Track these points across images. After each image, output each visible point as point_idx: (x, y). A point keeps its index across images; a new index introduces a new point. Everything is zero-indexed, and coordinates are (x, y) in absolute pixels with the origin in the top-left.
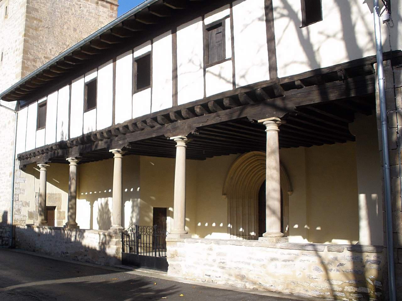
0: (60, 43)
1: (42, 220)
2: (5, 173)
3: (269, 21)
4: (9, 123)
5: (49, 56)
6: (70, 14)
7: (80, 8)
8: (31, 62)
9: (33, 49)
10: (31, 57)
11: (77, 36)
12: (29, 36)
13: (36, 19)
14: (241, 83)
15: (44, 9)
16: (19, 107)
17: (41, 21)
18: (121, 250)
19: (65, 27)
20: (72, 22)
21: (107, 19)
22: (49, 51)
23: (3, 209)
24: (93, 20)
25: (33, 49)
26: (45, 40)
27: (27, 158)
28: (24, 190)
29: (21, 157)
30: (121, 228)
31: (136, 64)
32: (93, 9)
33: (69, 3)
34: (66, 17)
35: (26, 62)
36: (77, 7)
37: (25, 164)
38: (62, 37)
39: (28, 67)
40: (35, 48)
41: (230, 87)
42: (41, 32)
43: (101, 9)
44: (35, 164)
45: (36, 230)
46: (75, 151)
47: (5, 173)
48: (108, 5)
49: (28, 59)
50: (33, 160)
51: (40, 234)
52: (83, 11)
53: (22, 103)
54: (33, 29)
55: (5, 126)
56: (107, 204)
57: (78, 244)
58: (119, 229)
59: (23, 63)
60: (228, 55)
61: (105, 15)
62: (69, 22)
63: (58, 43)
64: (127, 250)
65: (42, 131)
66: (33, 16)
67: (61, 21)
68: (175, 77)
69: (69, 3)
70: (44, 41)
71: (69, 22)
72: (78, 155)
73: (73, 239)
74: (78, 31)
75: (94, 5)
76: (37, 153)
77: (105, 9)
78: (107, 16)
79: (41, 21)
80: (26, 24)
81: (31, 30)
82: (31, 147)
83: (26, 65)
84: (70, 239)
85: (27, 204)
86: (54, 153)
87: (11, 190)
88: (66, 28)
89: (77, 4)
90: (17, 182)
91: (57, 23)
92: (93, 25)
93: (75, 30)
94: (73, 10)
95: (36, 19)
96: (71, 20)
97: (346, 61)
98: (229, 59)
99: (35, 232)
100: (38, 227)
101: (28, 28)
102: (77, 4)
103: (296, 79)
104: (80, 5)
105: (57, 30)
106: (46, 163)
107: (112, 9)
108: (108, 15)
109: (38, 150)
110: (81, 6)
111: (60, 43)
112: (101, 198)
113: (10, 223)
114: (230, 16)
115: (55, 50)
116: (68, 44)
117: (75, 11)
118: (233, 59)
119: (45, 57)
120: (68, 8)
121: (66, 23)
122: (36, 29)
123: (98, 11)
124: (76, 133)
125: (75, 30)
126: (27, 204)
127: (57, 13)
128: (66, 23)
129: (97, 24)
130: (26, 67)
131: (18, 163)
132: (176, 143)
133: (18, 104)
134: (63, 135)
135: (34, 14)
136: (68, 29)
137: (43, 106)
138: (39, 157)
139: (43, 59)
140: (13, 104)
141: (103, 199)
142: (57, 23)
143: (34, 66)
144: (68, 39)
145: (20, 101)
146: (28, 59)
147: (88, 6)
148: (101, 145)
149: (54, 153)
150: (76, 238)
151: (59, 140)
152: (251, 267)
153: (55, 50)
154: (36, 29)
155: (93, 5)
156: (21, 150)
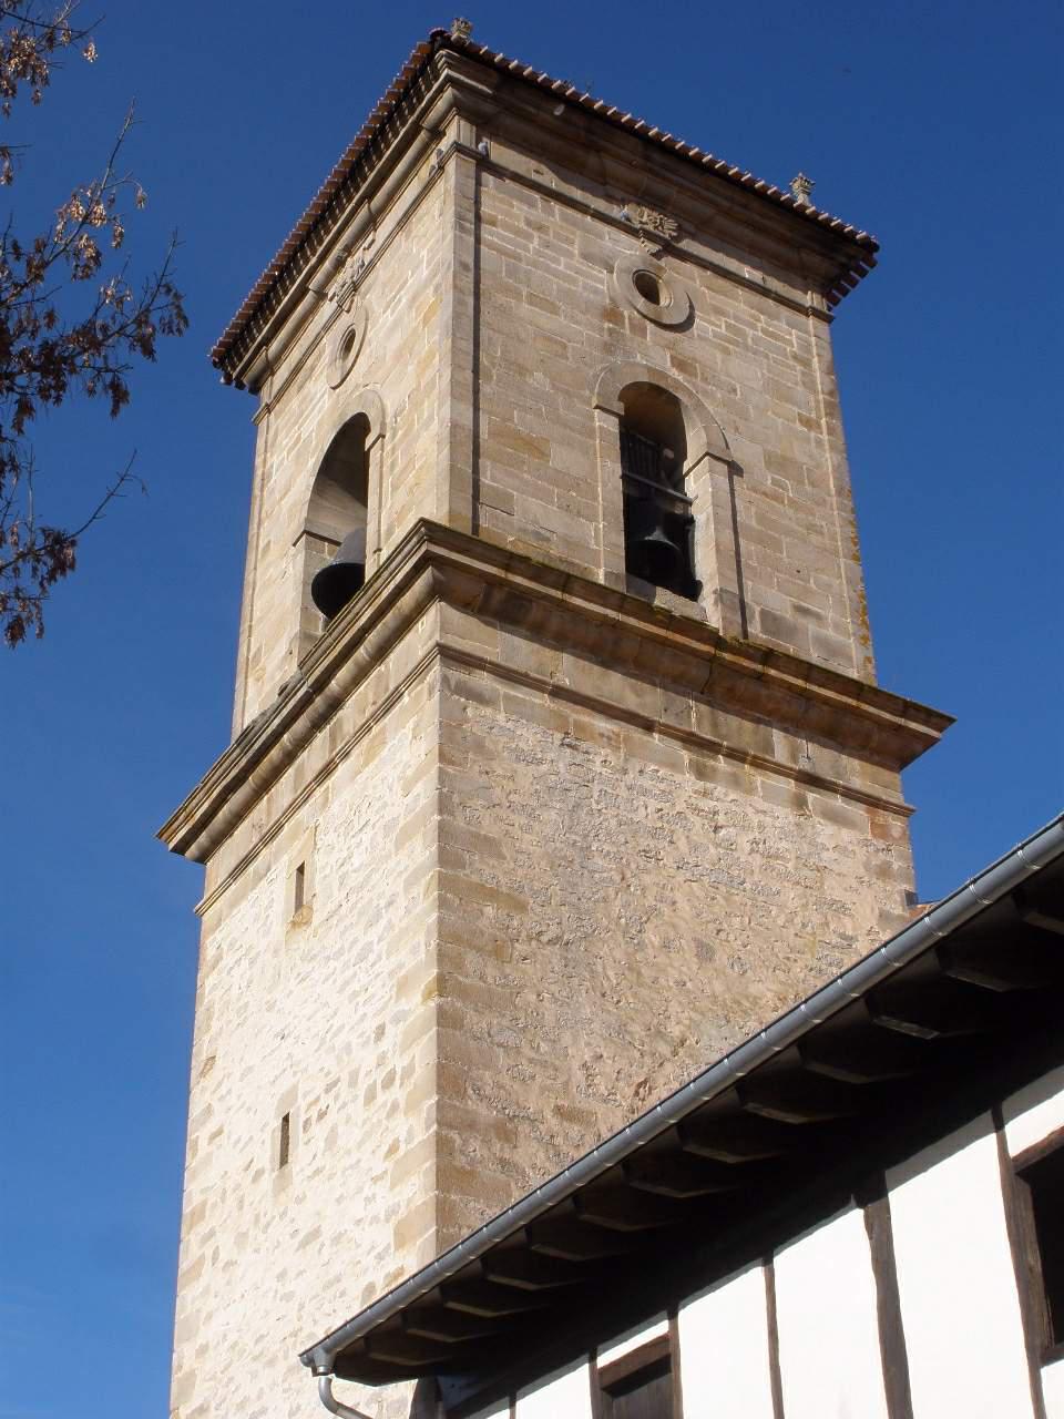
0: (637, 1029)
5: (582, 1103)
6: (669, 861)
7: (716, 829)
8: (486, 1142)
9: (488, 1065)
10: (485, 1113)
11: (718, 987)
12: (464, 993)
13: (493, 895)
15: (528, 842)
17: (522, 907)
19: (652, 937)
20: (683, 905)
21: (864, 890)
22: (579, 1075)
24: (791, 896)
25: (488, 1065)
26: (550, 1011)
32: (784, 835)
33: (653, 804)
34: (647, 879)
35: (458, 1141)
36: (698, 826)
38: (644, 992)
39: (472, 1174)
40: (502, 1060)
42: (527, 966)
43: (826, 832)
48: (858, 811)
49: (470, 1125)
52: (731, 846)
54: (479, 950)
59: (442, 1146)
61: (853, 866)
62: (666, 909)
63: (622, 1029)
66: (475, 878)
67: (626, 905)
69: (653, 804)
70: (549, 1018)
71: (666, 909)
74: (721, 958)
77: (846, 835)
78: (862, 871)
79: (522, 907)
80: (441, 921)
81: (472, 961)
83: (461, 1161)
88: (656, 941)
89: (697, 810)
91: (608, 916)
92: (798, 920)
93: (705, 952)
94: (682, 844)
95: (493, 895)
96: (678, 896)
101: (453, 945)
102: (697, 810)
104: (715, 813)
105: (612, 952)
107: (881, 831)
108: (867, 866)
110: (721, 819)
111: (637, 1029)
115: (608, 1067)
116: (675, 1031)
117: (695, 848)
119: (558, 1110)
120: (654, 833)
121: (652, 912)
122: (498, 951)
123: (812, 843)
125: (705, 952)
127: (600, 862)
128: (652, 912)
129: (816, 919)
130: (462, 1172)
135: (483, 870)
136: (666, 946)
139: (553, 1122)
142: (608, 916)
143: (503, 1163)
144: (674, 1008)
145: (444, 1381)
146: (470, 1125)
147: (755, 819)
153: (608, 1067)
154: (498, 951)
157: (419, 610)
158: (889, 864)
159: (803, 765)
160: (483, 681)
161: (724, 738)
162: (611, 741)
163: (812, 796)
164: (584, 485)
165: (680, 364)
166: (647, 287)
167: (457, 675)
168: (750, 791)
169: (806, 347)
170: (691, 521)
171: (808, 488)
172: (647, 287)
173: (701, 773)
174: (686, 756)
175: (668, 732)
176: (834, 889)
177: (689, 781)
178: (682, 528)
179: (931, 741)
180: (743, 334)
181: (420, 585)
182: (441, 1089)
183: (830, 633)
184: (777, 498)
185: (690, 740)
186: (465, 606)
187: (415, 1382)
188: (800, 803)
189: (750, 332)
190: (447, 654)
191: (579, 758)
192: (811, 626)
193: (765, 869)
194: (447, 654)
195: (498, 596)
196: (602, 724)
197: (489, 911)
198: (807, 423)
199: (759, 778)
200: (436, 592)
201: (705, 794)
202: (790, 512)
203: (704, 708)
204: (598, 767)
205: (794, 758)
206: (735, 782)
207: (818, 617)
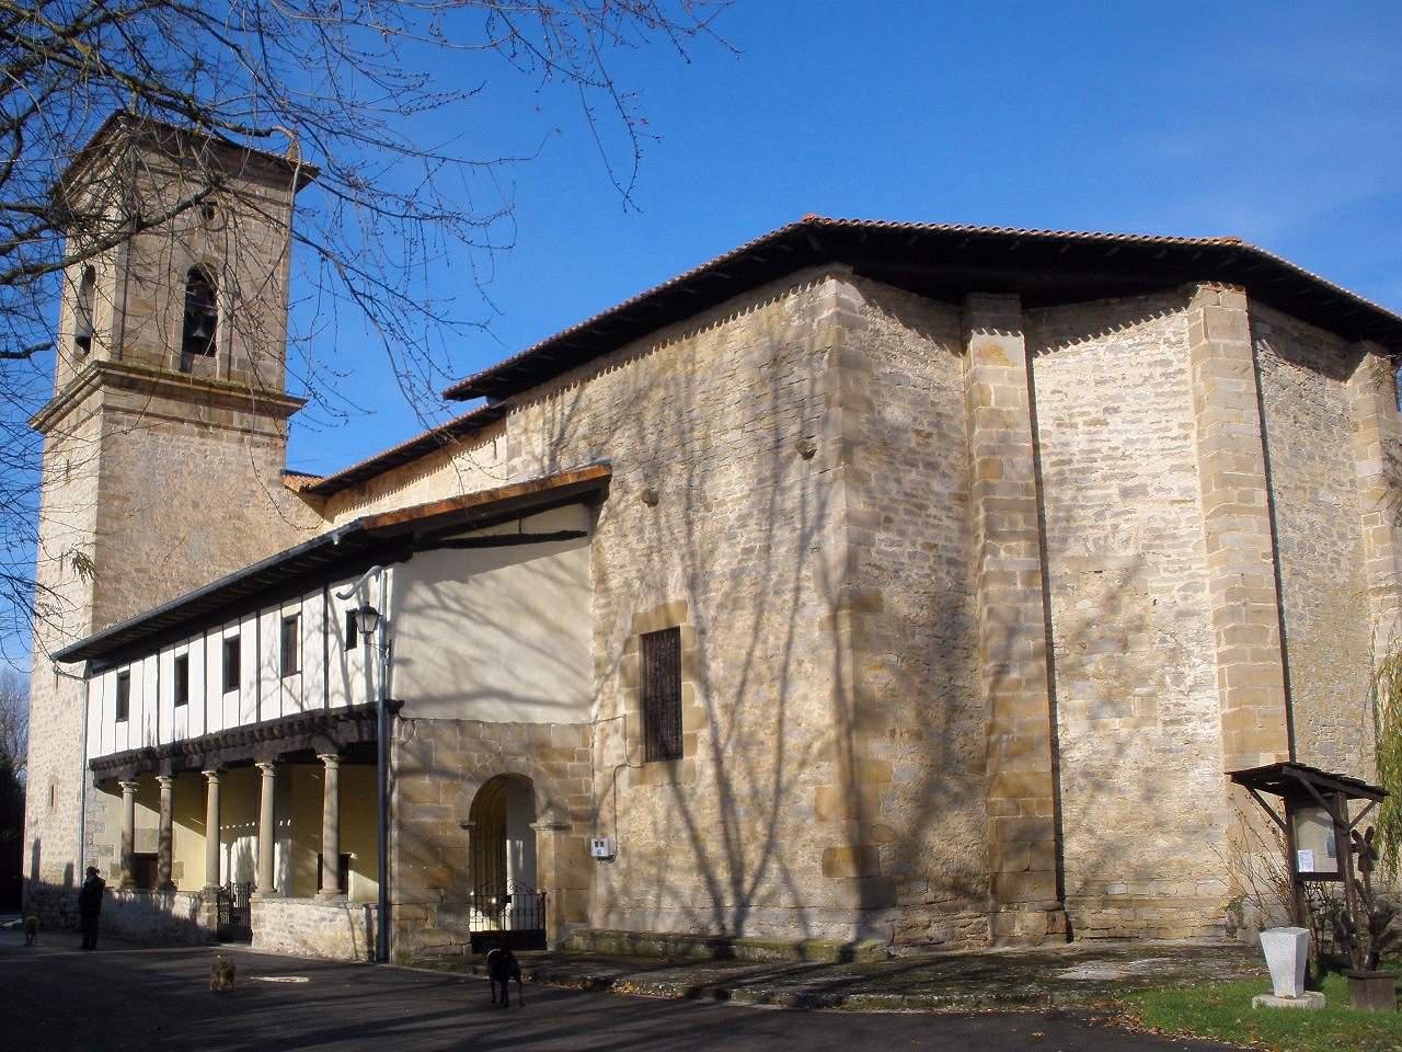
0: (167, 537)
1: (125, 878)
2: (69, 793)
3: (326, 634)
6: (185, 473)
8: (110, 584)
9: (114, 558)
10: (111, 573)
11: (200, 517)
13: (118, 498)
14: (306, 708)
15: (132, 474)
16: (92, 672)
17: (128, 500)
18: (216, 920)
19: (176, 503)
22: (145, 556)
23: (66, 859)
24: (232, 479)
25: (114, 558)
26: (135, 535)
27: (105, 769)
28: (102, 825)
29: (97, 765)
30: (216, 886)
31: (228, 647)
32: (233, 455)
33: (182, 451)
34: (176, 481)
37: (102, 777)
38: (170, 524)
40: (117, 555)
41: (297, 710)
43: (248, 450)
44: (116, 779)
45: (117, 895)
46: (166, 764)
47: (69, 793)
50: (113, 772)
51: (121, 903)
52: (211, 462)
53: (96, 666)
54: (111, 518)
55: (69, 703)
56: (249, 847)
57: (168, 912)
58: (214, 889)
60: (299, 669)
64: (226, 920)
66: (111, 492)
68: (259, 681)
69: (182, 451)
72: (170, 773)
73: (162, 907)
74: (202, 507)
75: (234, 447)
76: (117, 763)
79: (128, 500)
81: (109, 522)
82: (108, 750)
84: (159, 907)
85: (109, 851)
86: (141, 765)
87: (79, 825)
88: (177, 504)
89: (199, 451)
92: (234, 488)
93: (196, 505)
95: (118, 498)
96: (188, 486)
97: (365, 702)
98: (299, 672)
99: (115, 900)
100: (118, 891)
102: (199, 451)
103: (339, 712)
104: (206, 450)
105: (160, 511)
106: (132, 780)
108: (266, 462)
109: (119, 756)
111: (167, 537)
112: (241, 836)
113: (51, 881)
114: (300, 613)
115: (155, 552)
116: (181, 535)
118: (301, 672)
119: (136, 570)
120: (181, 463)
121: (177, 494)
122: (118, 517)
124: (166, 740)
125: (196, 505)
126: (109, 851)
128: (177, 494)
129: (242, 485)
131: (90, 775)
132: (262, 772)
133: (89, 666)
134: (149, 737)
135: (118, 489)
136: (181, 505)
137: (124, 680)
138: (121, 769)
139: (134, 574)
140: (79, 667)
141: (244, 839)
145: (94, 661)
146: (105, 579)
148: (196, 760)
149: (141, 765)
150: (165, 905)
151: (145, 746)
152: (310, 931)
153: (155, 552)
154: (118, 517)
155: (233, 445)
156: (93, 754)
157: (96, 388)
158: (274, 460)
159: (245, 425)
160: (119, 415)
161: (214, 419)
163: (247, 437)
168: (222, 439)
170: (217, 318)
173: (202, 435)
174: (196, 429)
175: (190, 422)
177: (198, 440)
178: (211, 324)
179: (298, 409)
185: (199, 424)
186: (114, 386)
187: (85, 662)
190: (106, 408)
193: (223, 470)
194: (106, 408)
195: (125, 382)
197: (116, 503)
199: (225, 434)
200: (103, 382)
201: (203, 444)
203: (206, 408)
204: (161, 441)
205: (241, 423)
206: (216, 437)
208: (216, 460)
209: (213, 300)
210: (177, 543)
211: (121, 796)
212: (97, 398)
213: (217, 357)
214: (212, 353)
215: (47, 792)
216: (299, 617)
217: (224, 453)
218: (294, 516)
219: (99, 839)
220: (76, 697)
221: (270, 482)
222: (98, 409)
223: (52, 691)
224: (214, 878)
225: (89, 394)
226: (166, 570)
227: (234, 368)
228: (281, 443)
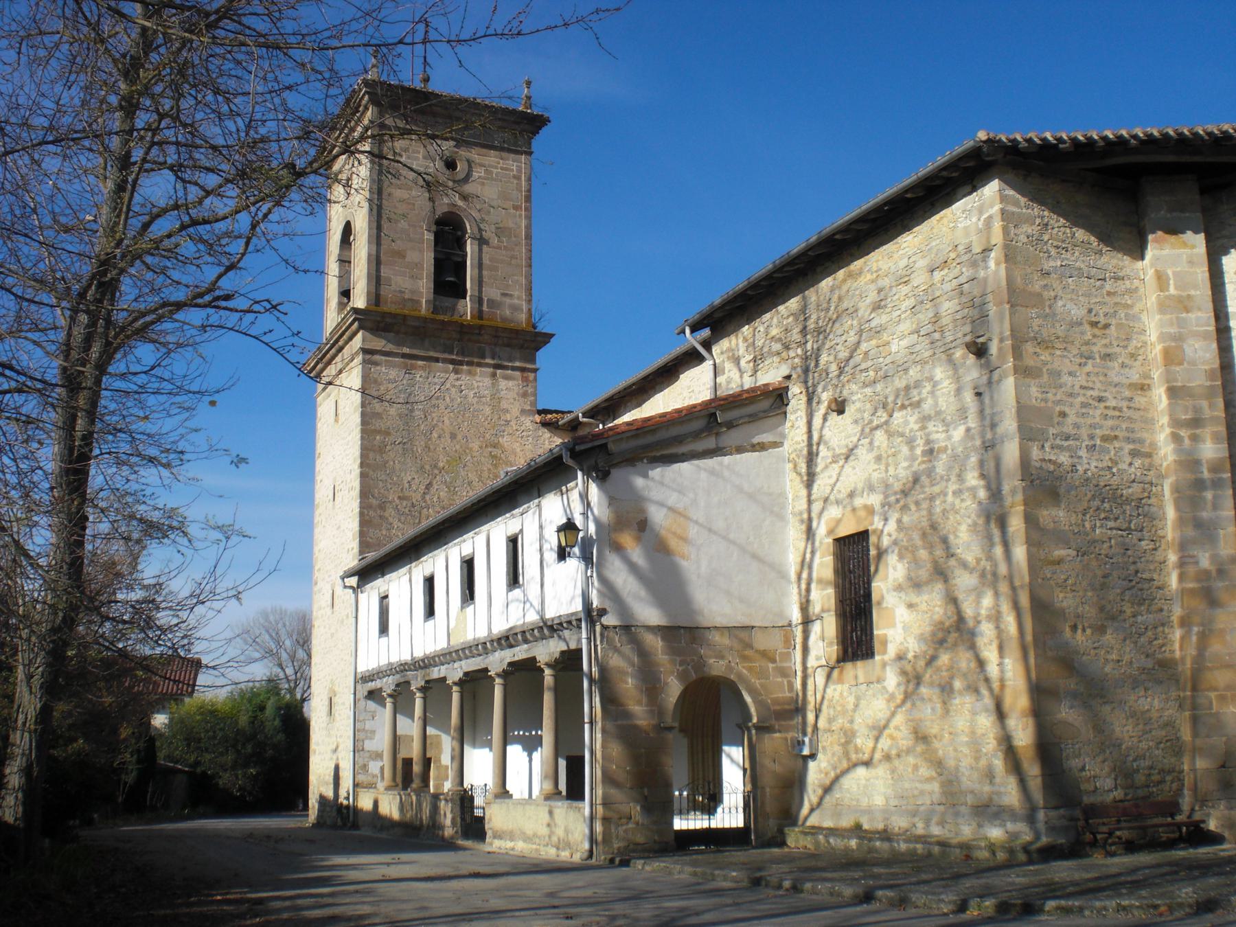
0: (427, 467)
4: (347, 616)
5: (407, 494)
7: (462, 391)
10: (374, 502)
11: (458, 447)
12: (368, 466)
13: (379, 432)
19: (435, 435)
20: (447, 422)
26: (397, 466)
28: (373, 732)
31: (465, 565)
32: (487, 388)
34: (434, 415)
39: (371, 521)
42: (390, 453)
43: (503, 384)
48: (518, 373)
49: (370, 507)
52: (466, 397)
54: (374, 451)
55: (342, 622)
61: (512, 395)
62: (440, 424)
63: (422, 467)
65: (384, 640)
71: (440, 424)
74: (459, 437)
77: (511, 383)
80: (362, 444)
81: (371, 455)
89: (454, 386)
90: (361, 718)
93: (453, 436)
94: (448, 399)
101: (366, 450)
102: (454, 386)
105: (419, 445)
107: (525, 379)
110: (463, 387)
115: (417, 481)
116: (441, 465)
117: (452, 400)
125: (453, 436)
129: (496, 417)
135: (377, 424)
139: (397, 501)
143: (381, 517)
144: (441, 457)
147: (476, 385)
157: (355, 334)
160: (377, 357)
162: (423, 368)
163: (499, 371)
164: (419, 266)
165: (464, 197)
166: (451, 165)
167: (368, 357)
169: (519, 171)
171: (514, 239)
172: (451, 165)
173: (456, 372)
174: (451, 367)
176: (504, 404)
177: (453, 376)
180: (491, 173)
181: (356, 324)
182: (361, 497)
183: (516, 301)
184: (499, 248)
188: (494, 375)
189: (495, 171)
191: (411, 376)
192: (508, 300)
194: (365, 351)
196: (420, 363)
197: (378, 437)
198: (516, 208)
199: (478, 370)
200: (360, 328)
201: (458, 379)
202: (504, 252)
204: (418, 379)
206: (470, 373)
207: (511, 296)
208: (471, 394)
209: (461, 245)
210: (436, 471)
211: (384, 706)
212: (357, 342)
213: (468, 298)
214: (463, 295)
215: (327, 703)
216: (520, 536)
217: (478, 387)
218: (547, 442)
219: (369, 745)
220: (347, 617)
221: (523, 411)
222: (357, 353)
223: (329, 610)
224: (458, 780)
225: (351, 339)
226: (427, 497)
227: (485, 308)
228: (531, 376)
